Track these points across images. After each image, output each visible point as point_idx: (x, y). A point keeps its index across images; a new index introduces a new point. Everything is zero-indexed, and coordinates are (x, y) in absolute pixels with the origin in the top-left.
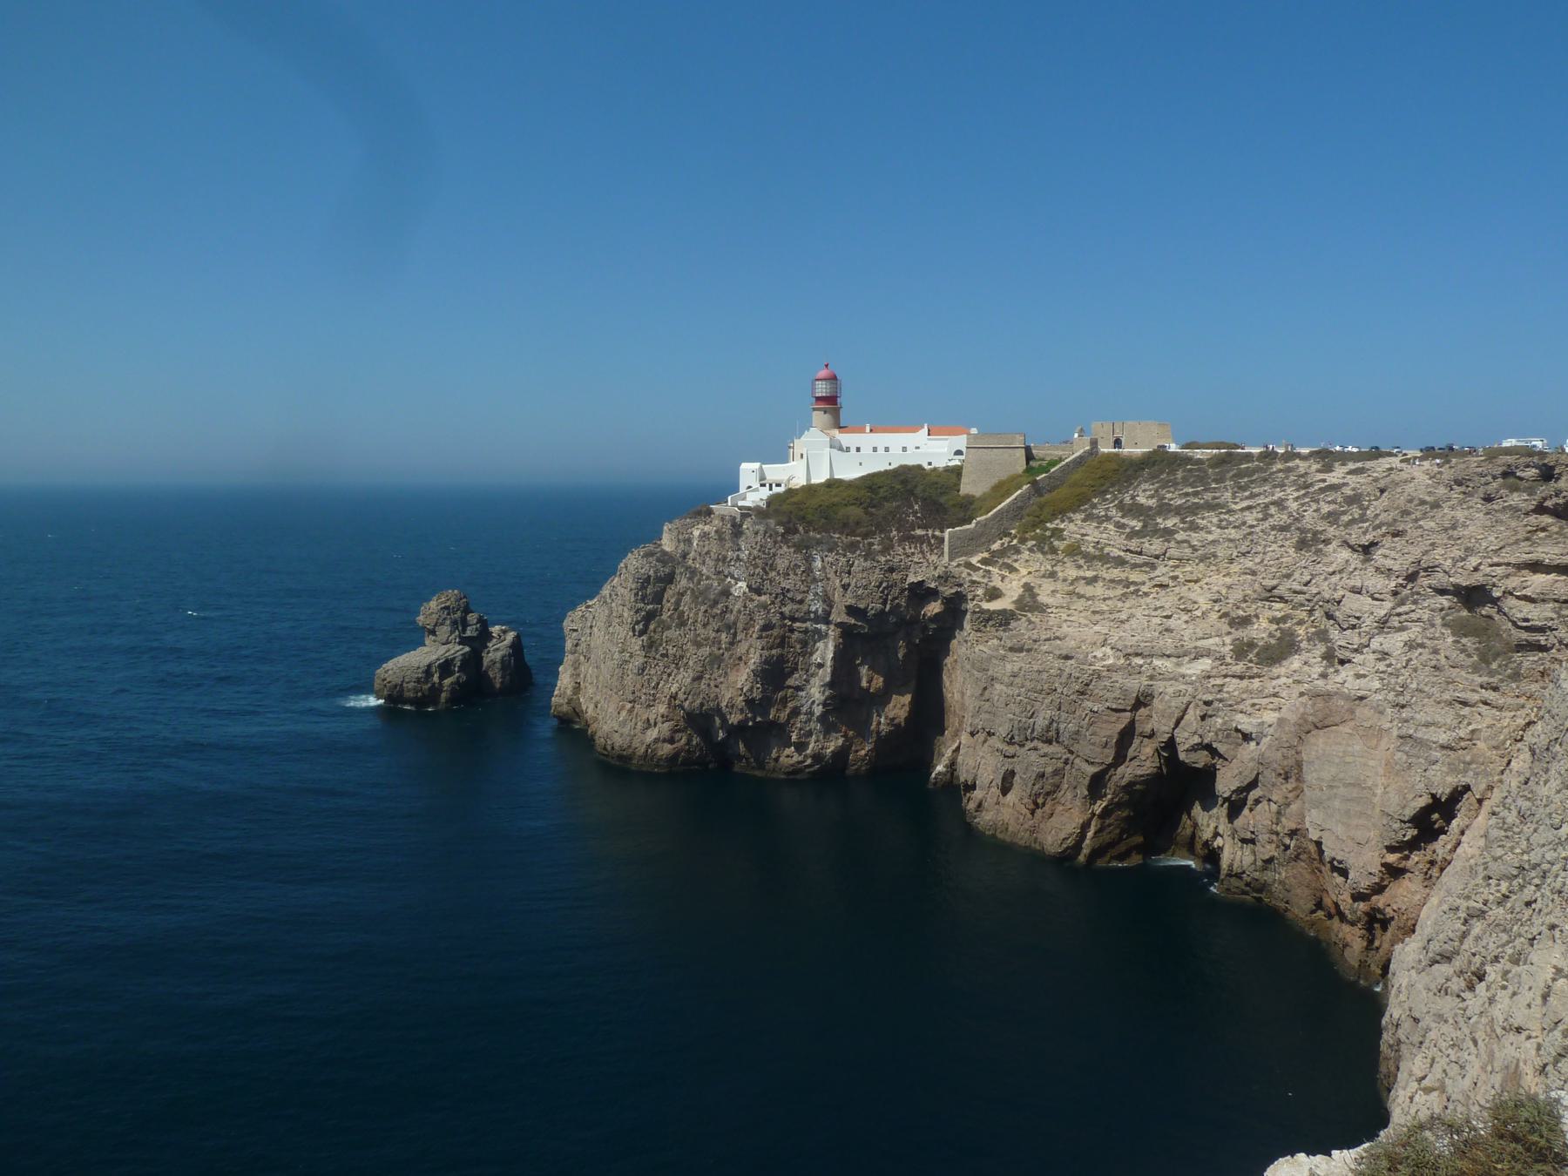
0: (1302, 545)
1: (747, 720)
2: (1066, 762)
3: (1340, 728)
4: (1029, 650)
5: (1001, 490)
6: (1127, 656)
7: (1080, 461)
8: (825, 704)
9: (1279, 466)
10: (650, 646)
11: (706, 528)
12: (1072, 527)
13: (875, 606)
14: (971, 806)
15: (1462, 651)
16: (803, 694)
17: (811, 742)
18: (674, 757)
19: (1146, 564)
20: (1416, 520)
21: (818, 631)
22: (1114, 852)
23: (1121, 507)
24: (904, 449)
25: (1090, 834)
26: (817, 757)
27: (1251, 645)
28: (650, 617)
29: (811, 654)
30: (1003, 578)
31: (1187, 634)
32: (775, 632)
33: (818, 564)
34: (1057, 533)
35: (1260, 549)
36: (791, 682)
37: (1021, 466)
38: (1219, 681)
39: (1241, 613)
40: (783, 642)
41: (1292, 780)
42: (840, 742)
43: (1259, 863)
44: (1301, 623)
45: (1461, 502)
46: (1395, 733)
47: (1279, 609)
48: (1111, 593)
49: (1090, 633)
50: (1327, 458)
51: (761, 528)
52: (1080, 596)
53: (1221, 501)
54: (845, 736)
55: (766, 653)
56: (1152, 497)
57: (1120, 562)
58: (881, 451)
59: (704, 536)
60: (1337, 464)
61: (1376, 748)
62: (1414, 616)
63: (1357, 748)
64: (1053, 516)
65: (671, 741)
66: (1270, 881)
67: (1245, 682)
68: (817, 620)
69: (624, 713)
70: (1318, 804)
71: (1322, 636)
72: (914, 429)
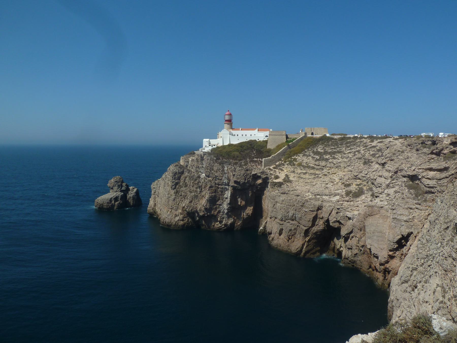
0: (365, 163)
1: (205, 214)
2: (298, 226)
3: (376, 216)
4: (287, 194)
5: (279, 147)
6: (315, 195)
7: (302, 139)
8: (228, 209)
9: (359, 141)
10: (177, 193)
11: (193, 158)
12: (299, 158)
13: (242, 181)
14: (270, 239)
15: (410, 194)
16: (221, 206)
17: (224, 221)
18: (183, 225)
19: (321, 169)
20: (397, 156)
21: (226, 188)
22: (312, 252)
23: (313, 152)
24: (251, 135)
25: (305, 247)
26: (225, 225)
27: (351, 192)
28: (177, 184)
29: (224, 195)
30: (280, 173)
31: (332, 189)
32: (213, 188)
33: (226, 168)
34: (295, 160)
35: (353, 164)
36: (218, 203)
37: (285, 140)
38: (341, 202)
39: (348, 183)
40: (215, 191)
41: (362, 231)
42: (232, 220)
43: (353, 255)
44: (365, 185)
45: (410, 151)
46: (391, 217)
47: (358, 182)
48: (310, 177)
49: (304, 189)
50: (372, 138)
51: (209, 158)
52: (302, 178)
53: (342, 150)
54: (234, 219)
55: (210, 194)
56: (322, 149)
57: (313, 168)
58: (244, 136)
59: (193, 160)
60: (375, 140)
61: (386, 221)
62: (397, 184)
63: (381, 221)
64: (294, 155)
65: (183, 220)
66: (356, 260)
67: (349, 203)
68: (226, 185)
69: (169, 212)
70: (370, 238)
71: (371, 189)
72: (254, 129)
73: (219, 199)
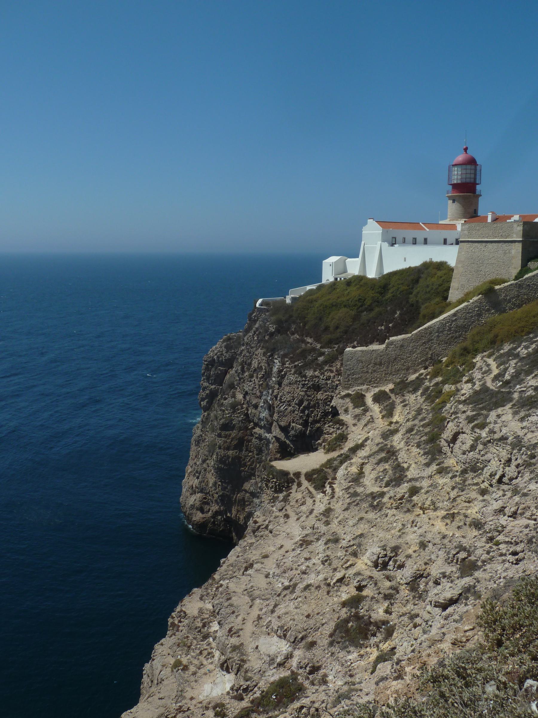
16: (256, 501)
18: (201, 526)
32: (234, 433)
36: (247, 486)
40: (240, 444)
55: (222, 452)
65: (202, 510)
73: (251, 475)
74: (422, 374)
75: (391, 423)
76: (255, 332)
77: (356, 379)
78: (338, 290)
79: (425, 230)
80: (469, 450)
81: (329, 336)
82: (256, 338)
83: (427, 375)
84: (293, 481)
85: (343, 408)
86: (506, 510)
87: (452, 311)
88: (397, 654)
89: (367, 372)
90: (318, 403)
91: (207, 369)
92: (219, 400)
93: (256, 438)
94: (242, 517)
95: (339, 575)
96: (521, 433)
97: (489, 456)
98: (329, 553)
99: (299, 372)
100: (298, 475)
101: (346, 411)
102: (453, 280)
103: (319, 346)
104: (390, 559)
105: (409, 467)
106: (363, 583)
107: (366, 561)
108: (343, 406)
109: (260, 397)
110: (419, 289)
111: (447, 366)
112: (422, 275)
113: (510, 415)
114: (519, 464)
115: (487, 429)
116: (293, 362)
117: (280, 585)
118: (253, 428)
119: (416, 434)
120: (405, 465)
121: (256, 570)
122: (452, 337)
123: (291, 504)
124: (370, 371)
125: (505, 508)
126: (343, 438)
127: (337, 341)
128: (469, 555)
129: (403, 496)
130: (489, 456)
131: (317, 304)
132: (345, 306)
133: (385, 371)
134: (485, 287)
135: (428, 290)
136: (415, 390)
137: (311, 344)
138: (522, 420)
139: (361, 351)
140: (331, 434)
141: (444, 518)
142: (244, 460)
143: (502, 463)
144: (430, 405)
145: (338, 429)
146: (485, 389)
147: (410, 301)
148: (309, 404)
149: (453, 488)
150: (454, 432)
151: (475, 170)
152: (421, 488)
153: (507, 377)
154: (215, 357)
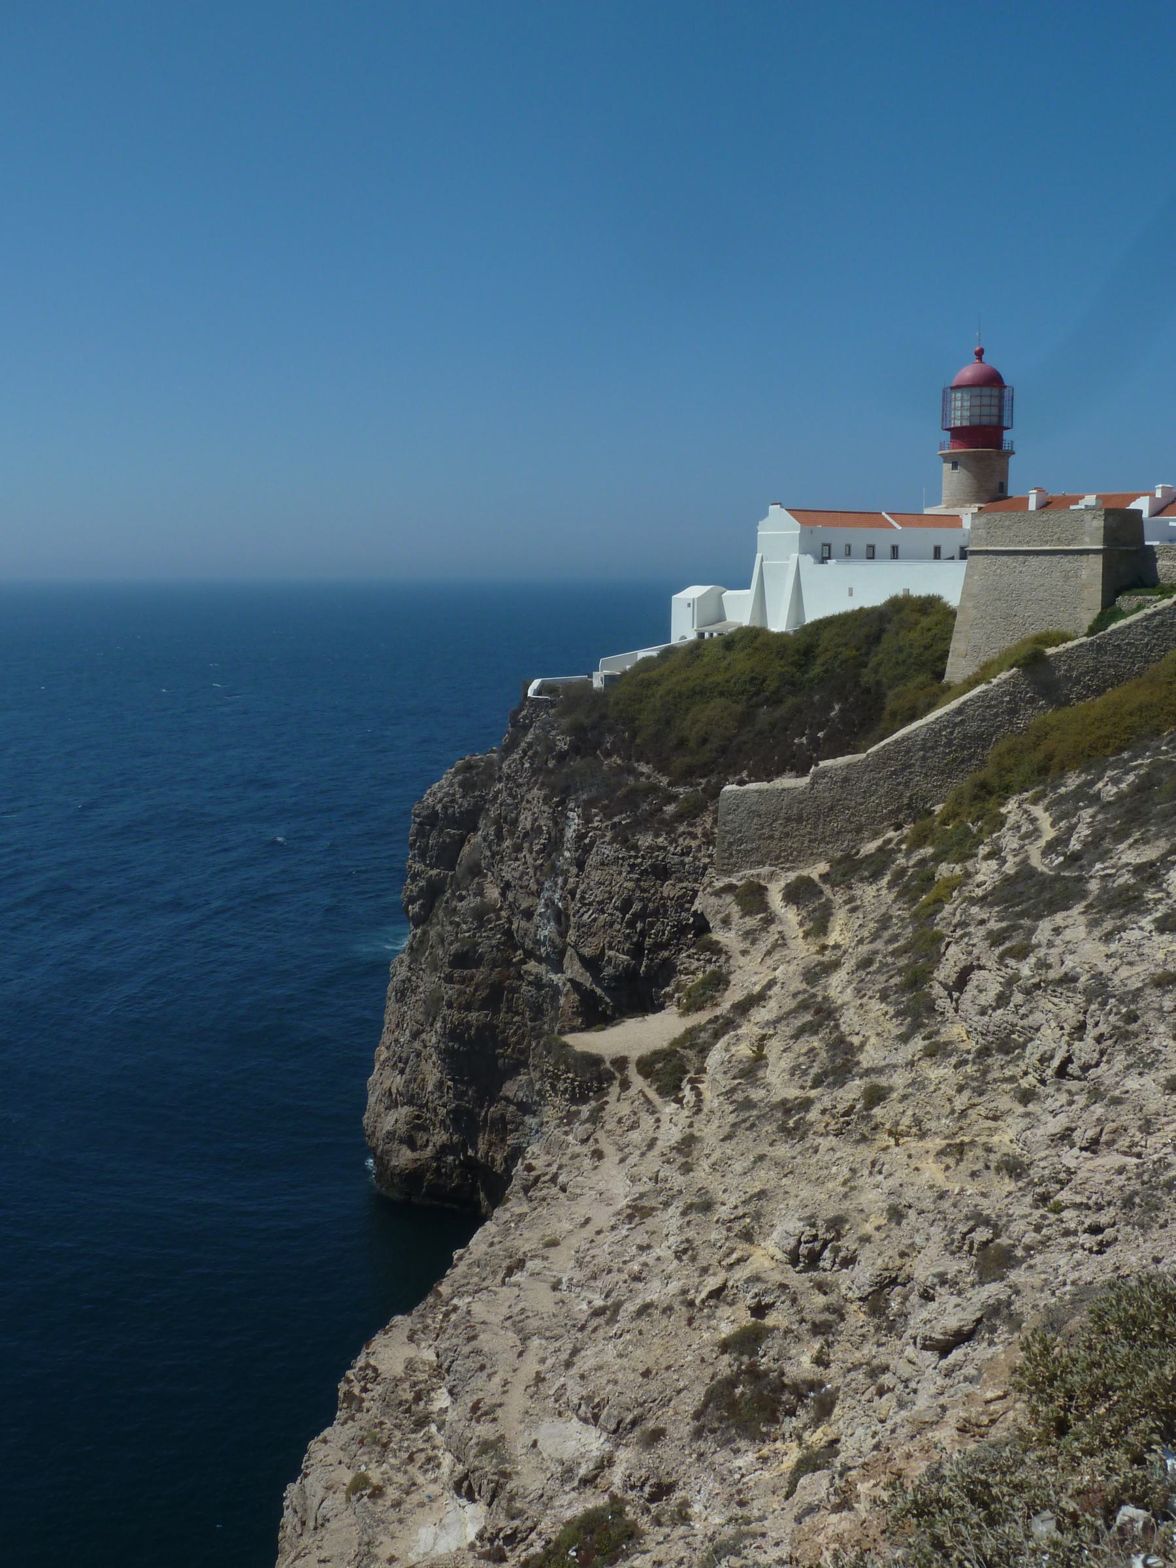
18: (413, 1177)
32: (480, 974)
36: (510, 1089)
40: (495, 996)
55: (455, 1016)
65: (411, 1144)
74: (890, 841)
75: (824, 948)
76: (525, 752)
77: (748, 853)
78: (706, 660)
79: (892, 526)
80: (994, 1004)
81: (688, 759)
82: (527, 765)
83: (901, 842)
84: (611, 1078)
85: (720, 916)
86: (1076, 1136)
87: (955, 704)
88: (842, 1454)
89: (771, 837)
90: (664, 905)
91: (421, 833)
92: (447, 902)
93: (530, 983)
94: (499, 1158)
95: (712, 1283)
96: (1105, 967)
97: (1037, 1018)
98: (690, 1233)
99: (623, 837)
100: (621, 1063)
101: (726, 922)
102: (955, 636)
103: (664, 781)
104: (824, 1246)
105: (863, 1044)
106: (768, 1299)
107: (773, 1250)
108: (718, 912)
109: (537, 894)
110: (880, 656)
111: (944, 822)
112: (888, 626)
113: (1082, 928)
114: (1102, 1035)
115: (1032, 960)
116: (610, 818)
117: (584, 1306)
118: (523, 962)
119: (878, 971)
120: (856, 1040)
121: (532, 1275)
122: (954, 760)
123: (608, 1127)
124: (777, 834)
125: (1073, 1130)
126: (719, 981)
127: (705, 770)
128: (997, 1235)
129: (853, 1107)
130: (1037, 1018)
131: (661, 690)
132: (722, 694)
133: (810, 833)
134: (1025, 651)
135: (901, 657)
136: (875, 877)
137: (648, 777)
138: (1108, 938)
139: (757, 791)
140: (693, 973)
141: (941, 1153)
142: (504, 1032)
143: (1065, 1032)
144: (909, 909)
145: (709, 961)
146: (1026, 872)
147: (864, 680)
148: (645, 907)
149: (960, 1089)
150: (961, 965)
151: (1001, 397)
152: (891, 1089)
153: (1075, 845)
154: (439, 807)
